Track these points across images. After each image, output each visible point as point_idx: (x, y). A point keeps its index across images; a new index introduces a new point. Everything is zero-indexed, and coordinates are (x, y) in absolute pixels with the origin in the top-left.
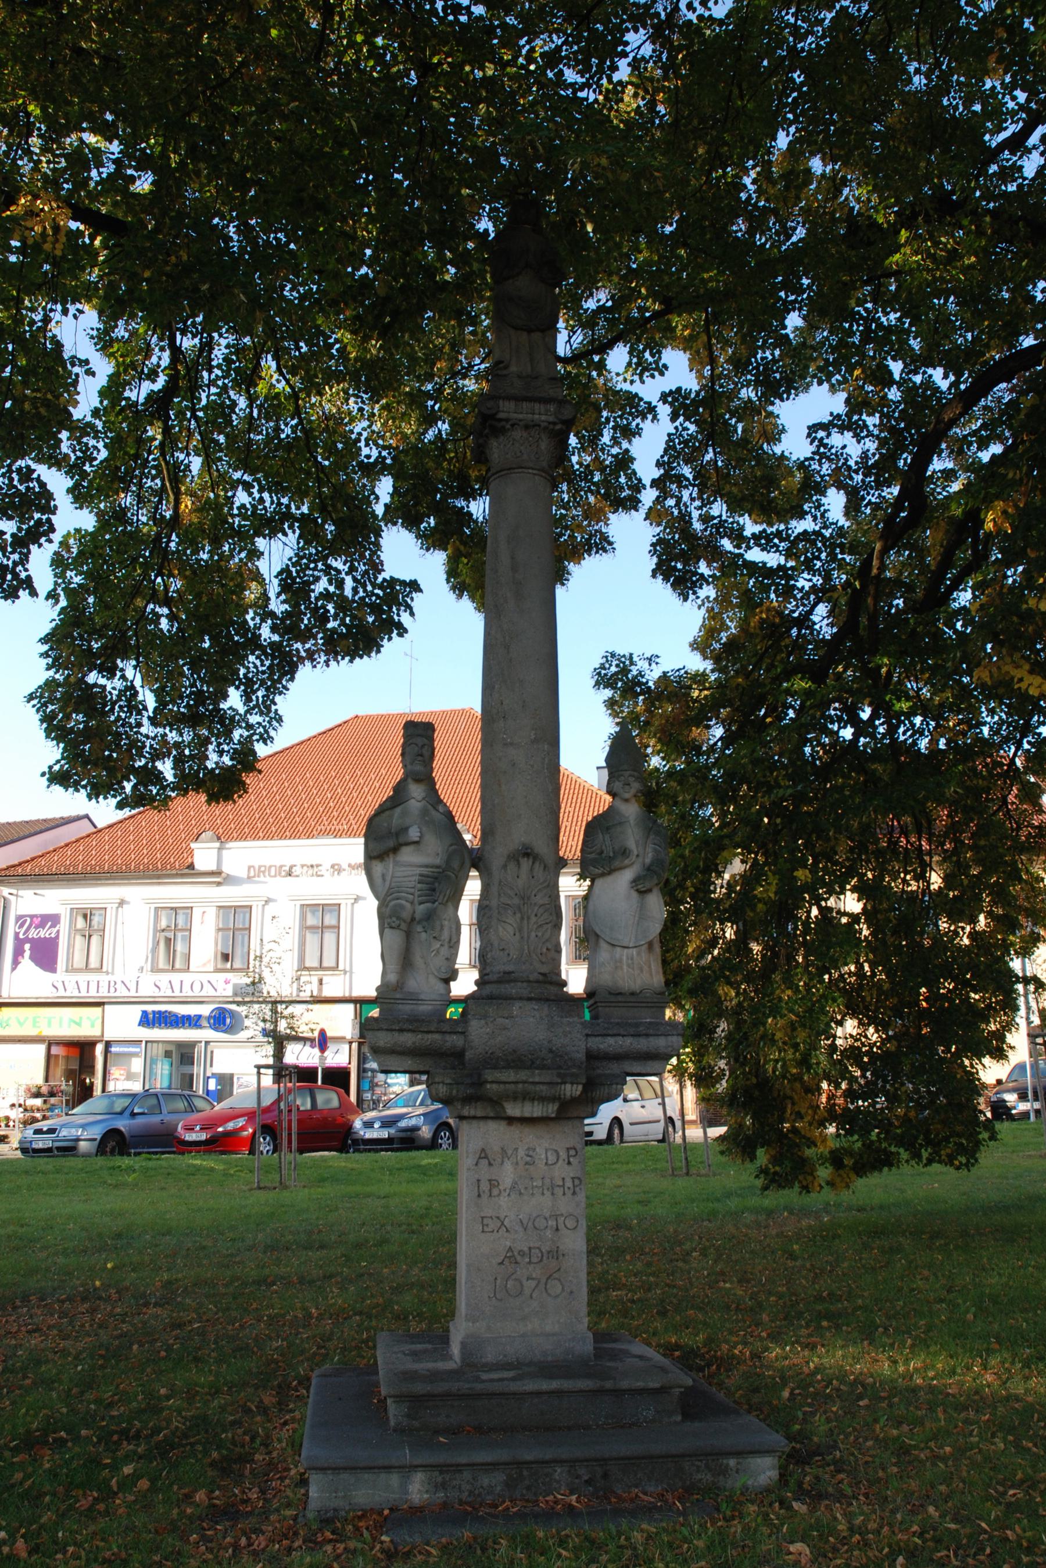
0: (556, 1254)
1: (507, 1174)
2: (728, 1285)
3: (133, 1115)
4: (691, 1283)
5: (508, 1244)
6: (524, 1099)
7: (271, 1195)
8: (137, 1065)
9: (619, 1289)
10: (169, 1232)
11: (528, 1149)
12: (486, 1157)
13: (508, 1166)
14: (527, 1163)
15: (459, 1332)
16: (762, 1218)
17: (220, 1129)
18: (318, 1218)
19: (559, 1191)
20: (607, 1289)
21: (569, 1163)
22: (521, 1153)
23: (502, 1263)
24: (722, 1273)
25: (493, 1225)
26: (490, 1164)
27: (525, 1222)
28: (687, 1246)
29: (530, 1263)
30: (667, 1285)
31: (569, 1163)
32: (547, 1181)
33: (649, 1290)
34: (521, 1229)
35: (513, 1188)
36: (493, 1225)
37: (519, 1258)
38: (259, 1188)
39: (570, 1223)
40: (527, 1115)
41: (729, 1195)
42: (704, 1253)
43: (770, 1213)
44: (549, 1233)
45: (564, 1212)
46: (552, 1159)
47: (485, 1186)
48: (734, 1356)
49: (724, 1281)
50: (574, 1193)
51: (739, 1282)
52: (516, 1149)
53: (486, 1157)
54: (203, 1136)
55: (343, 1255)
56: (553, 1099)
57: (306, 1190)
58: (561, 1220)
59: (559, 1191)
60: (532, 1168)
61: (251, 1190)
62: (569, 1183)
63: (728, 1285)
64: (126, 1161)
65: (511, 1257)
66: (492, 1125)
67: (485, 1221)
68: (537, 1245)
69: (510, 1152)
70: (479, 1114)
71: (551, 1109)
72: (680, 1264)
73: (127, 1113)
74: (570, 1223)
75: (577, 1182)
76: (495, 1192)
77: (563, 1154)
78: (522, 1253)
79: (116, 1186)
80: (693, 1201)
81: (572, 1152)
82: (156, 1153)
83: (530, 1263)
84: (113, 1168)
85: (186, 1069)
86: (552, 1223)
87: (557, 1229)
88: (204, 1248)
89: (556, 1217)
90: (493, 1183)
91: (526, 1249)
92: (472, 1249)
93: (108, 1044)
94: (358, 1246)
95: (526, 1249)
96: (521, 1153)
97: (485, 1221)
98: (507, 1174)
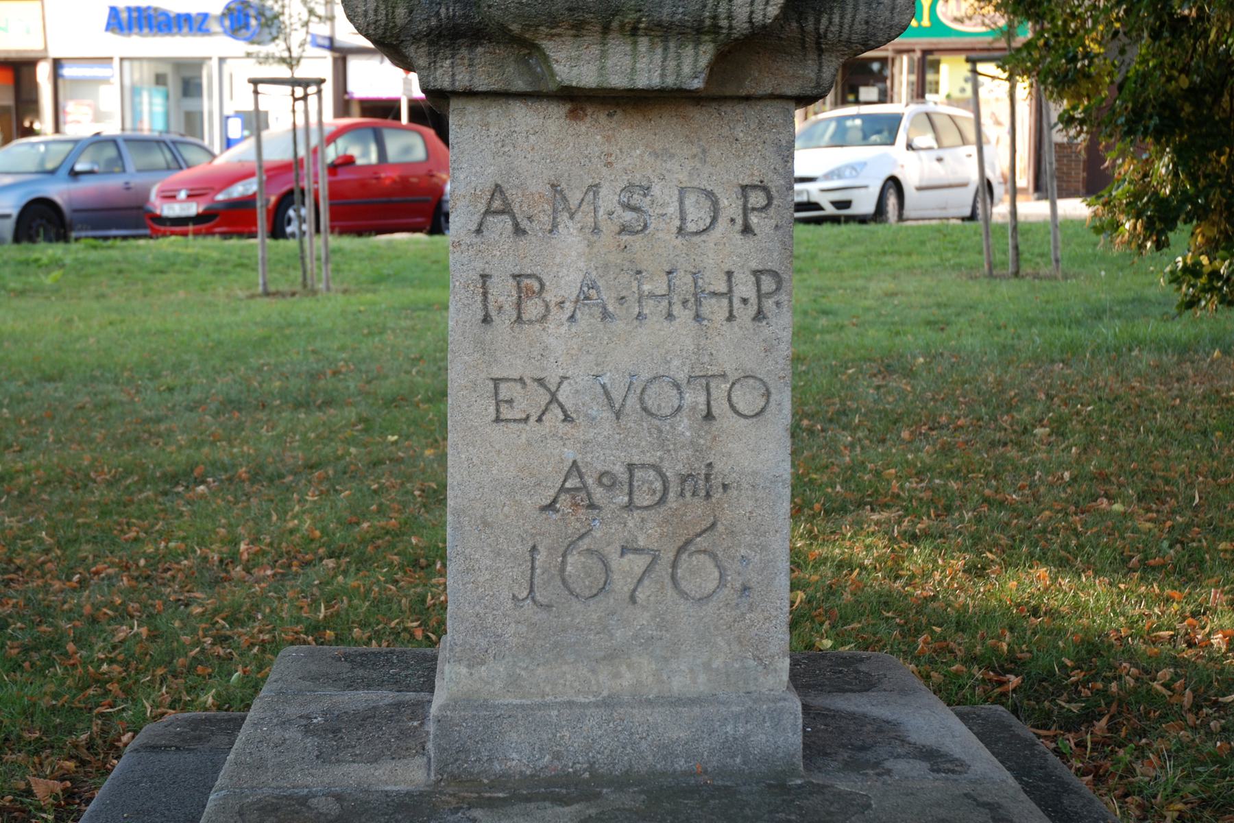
0: (703, 483)
1: (568, 259)
2: (1118, 507)
3: (74, 174)
4: (1036, 498)
5: (570, 454)
6: (606, 30)
7: (279, 305)
8: (109, 98)
9: (885, 506)
10: (60, 377)
11: (629, 188)
12: (506, 210)
13: (571, 237)
14: (623, 229)
15: (452, 679)
16: (1169, 359)
17: (220, 197)
18: (342, 348)
19: (716, 310)
20: (860, 505)
21: (747, 230)
22: (609, 198)
23: (551, 507)
24: (1103, 478)
25: (527, 401)
26: (519, 231)
27: (617, 395)
28: (1024, 415)
29: (630, 506)
30: (986, 500)
31: (747, 230)
32: (683, 281)
33: (948, 509)
34: (607, 414)
35: (584, 298)
36: (527, 401)
37: (598, 494)
38: (267, 294)
39: (747, 400)
40: (617, 81)
41: (1098, 314)
42: (1059, 429)
43: (1184, 350)
44: (684, 425)
45: (728, 368)
46: (697, 215)
47: (503, 292)
48: (1152, 696)
49: (1111, 498)
50: (760, 316)
51: (1141, 498)
52: (594, 188)
53: (506, 210)
54: (193, 209)
55: (361, 420)
56: (696, 31)
57: (340, 297)
58: (720, 390)
59: (716, 310)
60: (637, 242)
61: (252, 297)
62: (744, 287)
63: (1118, 507)
64: (54, 250)
65: (576, 492)
66: (523, 116)
67: (505, 391)
68: (648, 459)
69: (574, 197)
70: (482, 82)
71: (690, 66)
72: (1012, 452)
73: (64, 172)
74: (747, 400)
75: (768, 284)
76: (533, 309)
77: (730, 205)
78: (607, 480)
79: (21, 293)
80: (1031, 323)
81: (757, 199)
82: (125, 238)
83: (630, 506)
84: (26, 263)
85: (190, 104)
86: (694, 398)
87: (709, 416)
88: (109, 404)
89: (706, 381)
90: (527, 286)
91: (619, 470)
92: (488, 470)
93: (57, 64)
94: (395, 401)
95: (619, 470)
96: (609, 198)
97: (505, 391)
98: (568, 259)
